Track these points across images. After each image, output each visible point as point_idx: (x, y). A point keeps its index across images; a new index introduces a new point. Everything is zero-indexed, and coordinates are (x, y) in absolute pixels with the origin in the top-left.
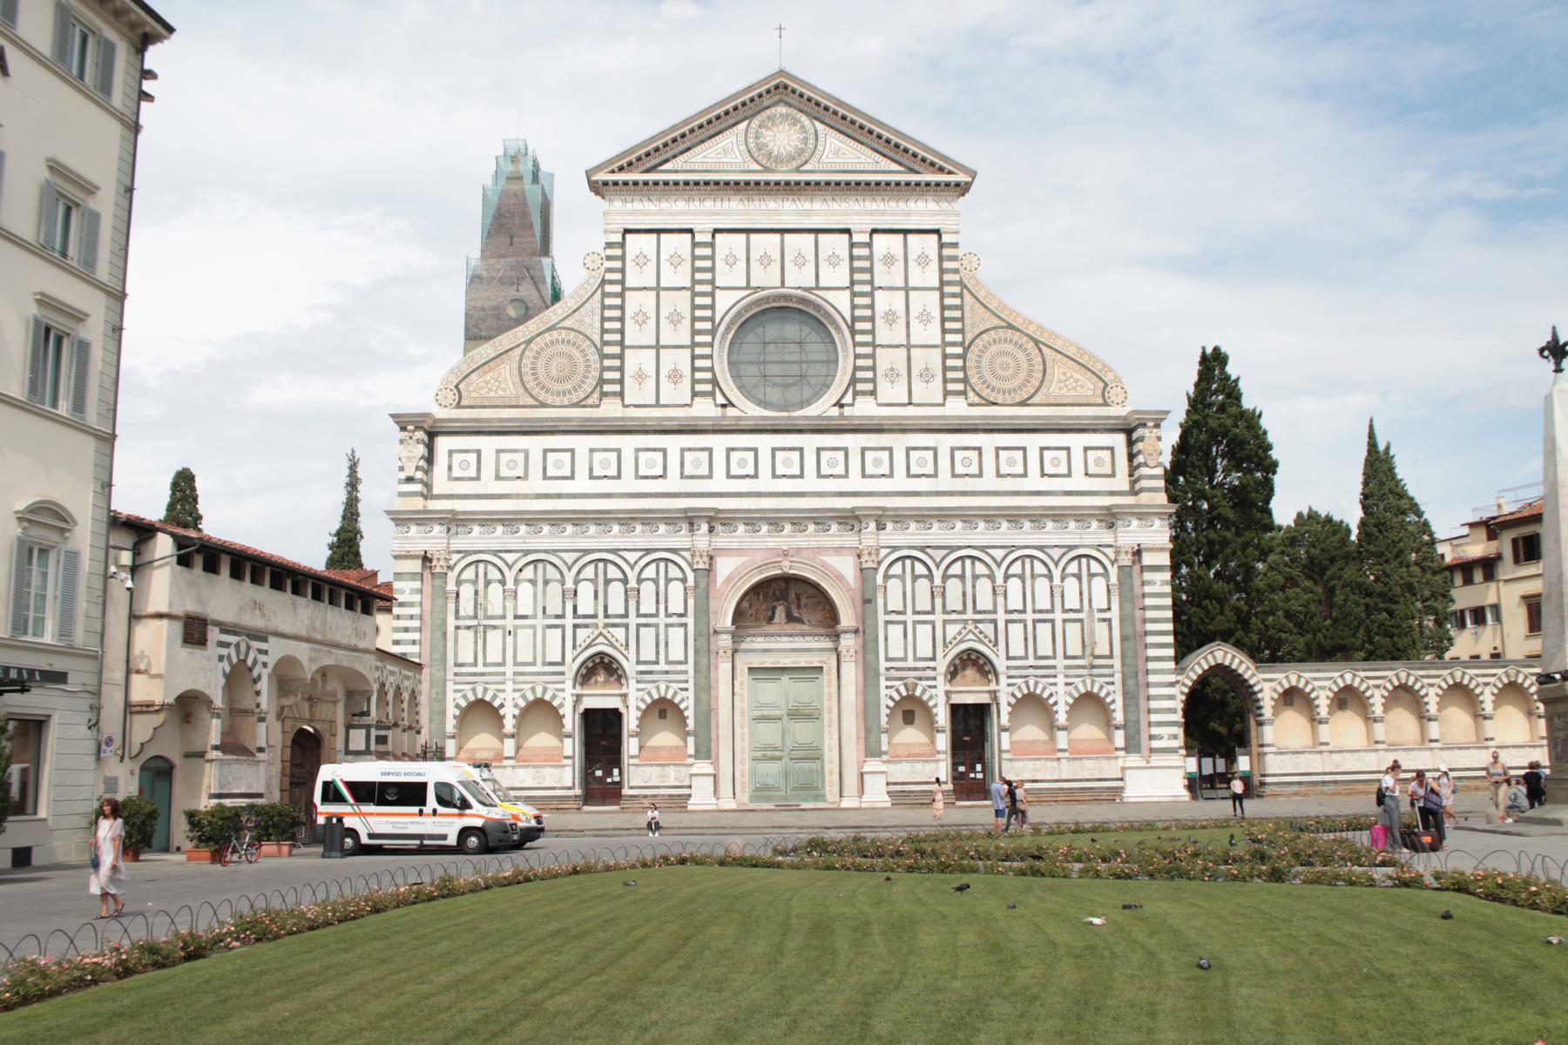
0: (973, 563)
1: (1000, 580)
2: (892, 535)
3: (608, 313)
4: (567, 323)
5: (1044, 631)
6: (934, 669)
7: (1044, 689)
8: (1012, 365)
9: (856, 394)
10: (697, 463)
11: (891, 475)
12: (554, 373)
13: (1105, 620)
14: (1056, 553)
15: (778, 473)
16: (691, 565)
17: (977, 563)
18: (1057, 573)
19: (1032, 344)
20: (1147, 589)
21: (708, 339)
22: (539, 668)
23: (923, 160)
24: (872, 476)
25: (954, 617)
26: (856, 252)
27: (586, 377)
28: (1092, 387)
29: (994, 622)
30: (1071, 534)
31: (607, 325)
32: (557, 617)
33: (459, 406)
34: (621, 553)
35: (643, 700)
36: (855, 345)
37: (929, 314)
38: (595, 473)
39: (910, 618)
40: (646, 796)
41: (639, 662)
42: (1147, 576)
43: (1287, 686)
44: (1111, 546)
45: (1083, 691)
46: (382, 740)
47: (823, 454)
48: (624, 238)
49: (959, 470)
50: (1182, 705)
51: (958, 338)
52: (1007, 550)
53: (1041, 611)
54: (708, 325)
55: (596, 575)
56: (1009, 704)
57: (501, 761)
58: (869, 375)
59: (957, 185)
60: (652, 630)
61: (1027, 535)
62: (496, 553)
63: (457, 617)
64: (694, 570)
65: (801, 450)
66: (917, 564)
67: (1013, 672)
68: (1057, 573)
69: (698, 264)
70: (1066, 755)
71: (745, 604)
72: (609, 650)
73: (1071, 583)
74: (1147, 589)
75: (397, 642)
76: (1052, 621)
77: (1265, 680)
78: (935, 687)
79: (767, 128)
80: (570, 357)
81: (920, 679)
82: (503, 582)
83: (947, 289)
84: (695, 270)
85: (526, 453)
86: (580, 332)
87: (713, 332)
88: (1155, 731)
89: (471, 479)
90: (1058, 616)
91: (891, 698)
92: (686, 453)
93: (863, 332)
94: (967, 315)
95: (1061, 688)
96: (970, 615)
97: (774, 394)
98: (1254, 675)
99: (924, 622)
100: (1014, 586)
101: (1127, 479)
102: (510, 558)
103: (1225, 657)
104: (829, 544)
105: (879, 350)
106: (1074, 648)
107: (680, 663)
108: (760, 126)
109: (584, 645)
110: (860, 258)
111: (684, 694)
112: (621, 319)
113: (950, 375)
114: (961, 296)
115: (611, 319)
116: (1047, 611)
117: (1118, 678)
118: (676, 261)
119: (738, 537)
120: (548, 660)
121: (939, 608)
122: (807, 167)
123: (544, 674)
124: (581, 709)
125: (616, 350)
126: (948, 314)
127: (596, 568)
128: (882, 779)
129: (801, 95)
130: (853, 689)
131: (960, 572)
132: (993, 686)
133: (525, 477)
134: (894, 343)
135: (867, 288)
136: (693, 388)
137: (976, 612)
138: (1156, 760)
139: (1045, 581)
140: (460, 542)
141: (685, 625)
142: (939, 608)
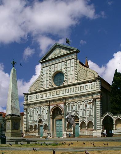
1: (79, 105)
49: (76, 90)
54: (50, 77)
83: (75, 66)
88: (98, 126)
95: (86, 121)
97: (58, 84)
100: (81, 106)
112: (43, 78)
114: (77, 66)
125: (42, 82)
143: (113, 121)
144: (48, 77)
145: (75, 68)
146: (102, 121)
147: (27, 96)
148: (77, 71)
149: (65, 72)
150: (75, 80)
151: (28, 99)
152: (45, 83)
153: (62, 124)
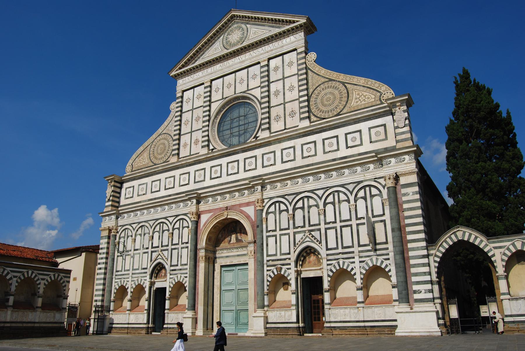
0: (308, 200)
1: (321, 207)
2: (269, 193)
4: (164, 132)
5: (346, 231)
6: (290, 259)
7: (348, 266)
8: (332, 98)
9: (263, 130)
12: (159, 151)
13: (381, 221)
14: (351, 187)
16: (190, 220)
17: (310, 199)
18: (352, 198)
19: (341, 85)
20: (404, 199)
27: (168, 150)
28: (373, 97)
29: (319, 230)
33: (132, 171)
35: (172, 283)
37: (293, 86)
40: (170, 328)
41: (171, 266)
42: (404, 191)
45: (371, 265)
49: (306, 154)
50: (436, 270)
52: (325, 190)
54: (207, 118)
55: (160, 229)
56: (329, 276)
57: (125, 312)
59: (301, 26)
61: (335, 180)
62: (130, 225)
63: (118, 252)
64: (191, 221)
66: (282, 205)
67: (330, 257)
68: (352, 198)
70: (362, 305)
71: (220, 236)
72: (162, 261)
73: (361, 203)
74: (404, 199)
76: (351, 226)
77: (495, 248)
78: (290, 269)
79: (230, 35)
80: (164, 144)
81: (283, 265)
82: (132, 236)
83: (300, 72)
85: (147, 184)
86: (168, 134)
87: (209, 121)
88: (415, 287)
90: (354, 222)
91: (270, 276)
94: (310, 81)
95: (357, 265)
96: (307, 228)
98: (486, 245)
99: (285, 234)
100: (329, 208)
102: (134, 226)
104: (244, 201)
105: (272, 109)
106: (365, 239)
109: (154, 260)
112: (180, 125)
114: (306, 73)
117: (391, 255)
121: (291, 226)
123: (141, 273)
127: (160, 225)
131: (302, 206)
137: (310, 225)
138: (417, 307)
140: (121, 222)
143: (492, 263)
144: (197, 120)
145: (299, 81)
146: (434, 270)
147: (119, 185)
148: (307, 89)
150: (301, 119)
151: (119, 198)
152: (185, 139)
153: (246, 283)
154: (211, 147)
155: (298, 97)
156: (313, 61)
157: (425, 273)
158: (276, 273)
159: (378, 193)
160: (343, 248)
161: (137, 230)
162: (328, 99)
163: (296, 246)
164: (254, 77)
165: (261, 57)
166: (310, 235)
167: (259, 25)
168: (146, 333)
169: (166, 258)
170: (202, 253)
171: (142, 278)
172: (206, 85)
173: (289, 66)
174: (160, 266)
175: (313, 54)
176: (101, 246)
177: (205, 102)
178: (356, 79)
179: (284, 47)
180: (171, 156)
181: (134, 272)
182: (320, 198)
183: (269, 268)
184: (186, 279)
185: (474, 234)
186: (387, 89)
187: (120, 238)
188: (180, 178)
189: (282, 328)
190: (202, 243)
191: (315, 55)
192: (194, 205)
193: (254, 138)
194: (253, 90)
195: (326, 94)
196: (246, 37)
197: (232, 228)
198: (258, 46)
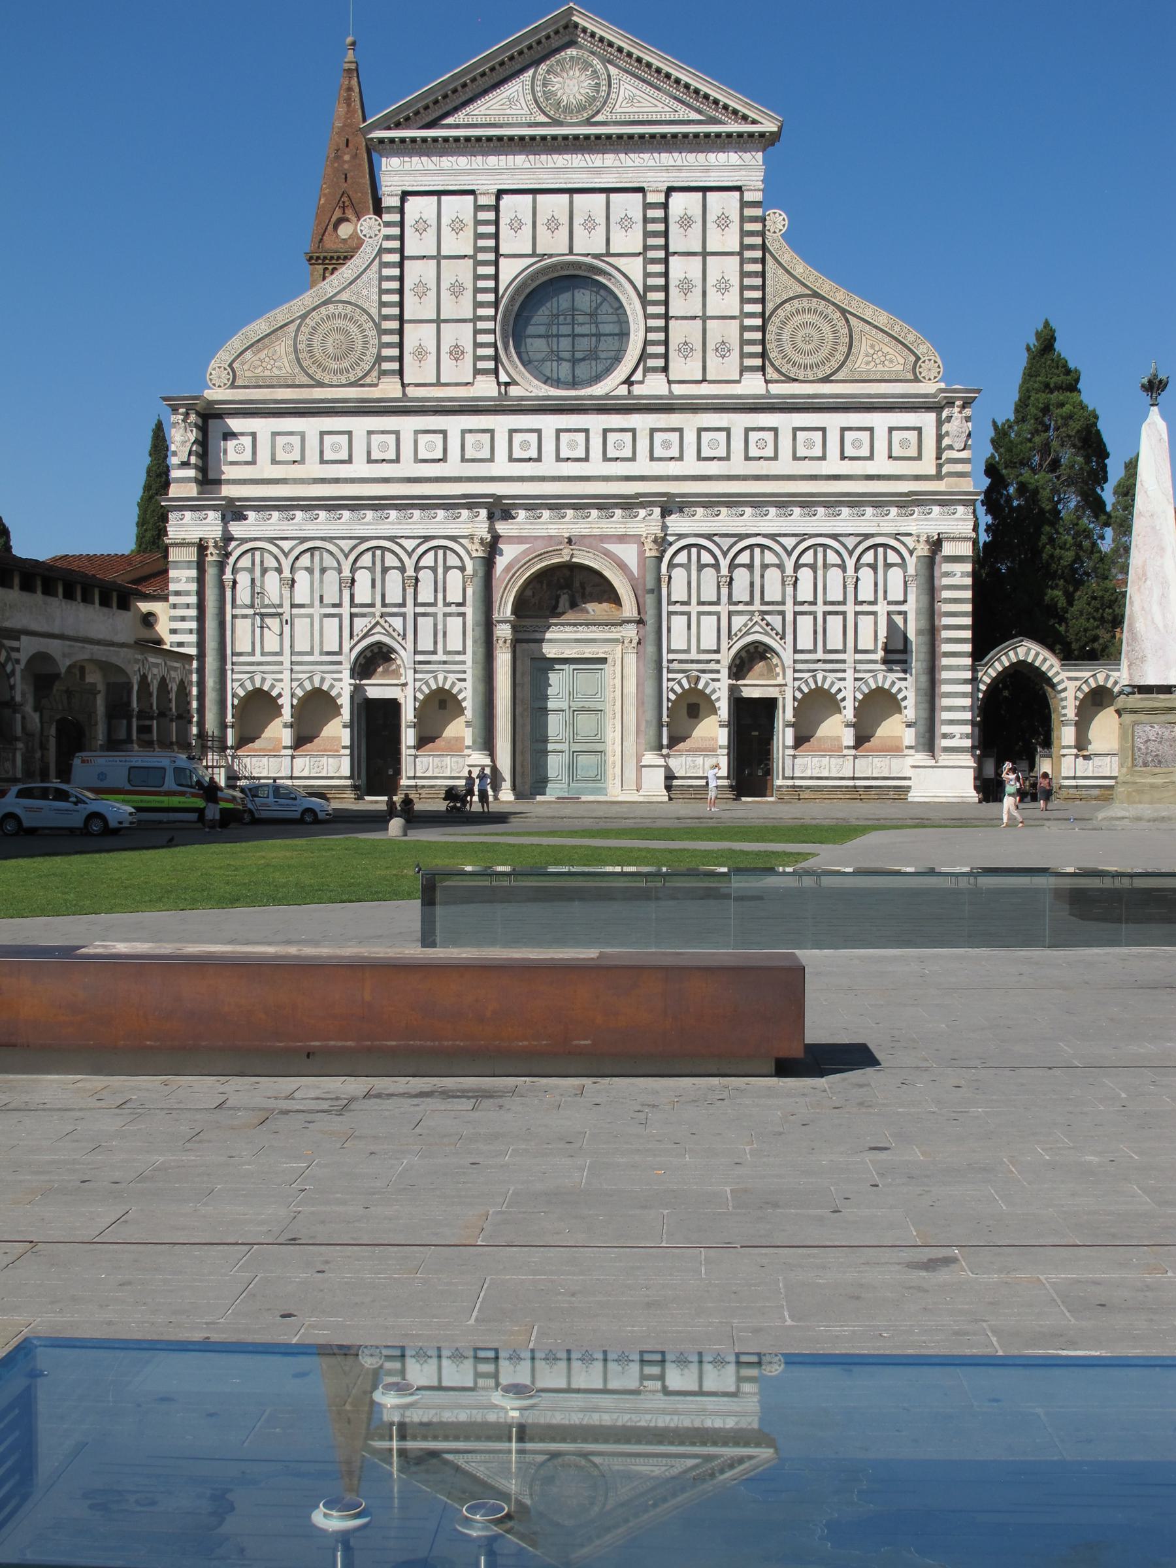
0: (762, 552)
1: (789, 570)
2: (676, 523)
3: (386, 285)
4: (344, 296)
5: (835, 623)
6: (718, 662)
7: (833, 684)
8: (816, 337)
9: (647, 370)
10: (478, 446)
11: (681, 458)
13: (900, 613)
14: (850, 542)
15: (562, 456)
18: (850, 563)
19: (838, 314)
21: (491, 312)
22: (316, 657)
23: (726, 107)
24: (660, 459)
25: (740, 608)
26: (651, 213)
27: (364, 354)
28: (902, 361)
29: (783, 613)
30: (869, 521)
31: (386, 298)
32: (334, 606)
33: (233, 386)
34: (398, 541)
35: (420, 690)
36: (647, 316)
38: (373, 458)
39: (694, 608)
40: (423, 786)
41: (416, 652)
42: (946, 567)
43: (1093, 685)
44: (910, 535)
45: (873, 686)
46: (145, 730)
47: (610, 436)
48: (403, 201)
51: (758, 308)
52: (799, 539)
53: (832, 603)
55: (374, 563)
56: (795, 699)
58: (661, 349)
59: (762, 135)
60: (431, 619)
61: (820, 522)
62: (271, 540)
63: (234, 606)
64: (472, 558)
65: (587, 431)
67: (799, 666)
68: (850, 563)
69: (482, 229)
70: (853, 752)
71: (529, 593)
72: (386, 640)
73: (866, 574)
74: (946, 581)
75: (174, 632)
76: (844, 613)
77: (1069, 679)
78: (718, 680)
79: (557, 75)
80: (347, 333)
81: (704, 671)
82: (279, 570)
83: (748, 254)
84: (478, 236)
85: (303, 436)
86: (357, 306)
87: (496, 304)
88: (945, 729)
89: (247, 463)
90: (850, 608)
92: (467, 436)
93: (655, 303)
95: (849, 683)
96: (757, 606)
97: (565, 370)
98: (1057, 673)
100: (805, 574)
101: (934, 462)
102: (286, 545)
103: (1027, 654)
105: (672, 323)
106: (866, 642)
107: (458, 653)
108: (548, 72)
110: (654, 220)
111: (462, 684)
112: (401, 291)
113: (748, 349)
114: (763, 261)
115: (389, 291)
116: (839, 603)
118: (457, 226)
119: (518, 523)
120: (325, 650)
121: (724, 599)
122: (599, 118)
123: (322, 663)
124: (356, 701)
125: (395, 325)
126: (747, 281)
127: (374, 556)
128: (661, 773)
129: (593, 35)
130: (634, 681)
132: (780, 680)
133: (302, 461)
134: (689, 315)
135: (661, 254)
136: (475, 365)
137: (763, 603)
138: (944, 759)
139: (838, 571)
141: (463, 615)
142: (724, 599)
149: (648, 289)
150: (743, 369)
154: (504, 378)
155: (737, 313)
156: (779, 234)
157: (964, 707)
158: (687, 686)
159: (900, 561)
160: (826, 651)
161: (297, 558)
162: (807, 339)
163: (732, 640)
164: (626, 223)
165: (650, 176)
166: (762, 620)
167: (644, 81)
168: (355, 799)
169: (399, 635)
170: (503, 632)
171: (325, 675)
172: (482, 201)
173: (719, 226)
174: (372, 651)
175: (780, 215)
176: (173, 587)
177: (478, 249)
178: (869, 311)
179: (712, 174)
180: (375, 373)
181: (295, 658)
182: (789, 554)
183: (671, 676)
184: (460, 685)
185: (1045, 653)
186: (930, 354)
187: (235, 571)
188: (416, 442)
189: (697, 786)
190: (505, 609)
191: (784, 220)
192: (482, 522)
193: (624, 383)
194: (623, 260)
195: (806, 324)
196: (605, 102)
197: (562, 581)
198: (642, 143)
